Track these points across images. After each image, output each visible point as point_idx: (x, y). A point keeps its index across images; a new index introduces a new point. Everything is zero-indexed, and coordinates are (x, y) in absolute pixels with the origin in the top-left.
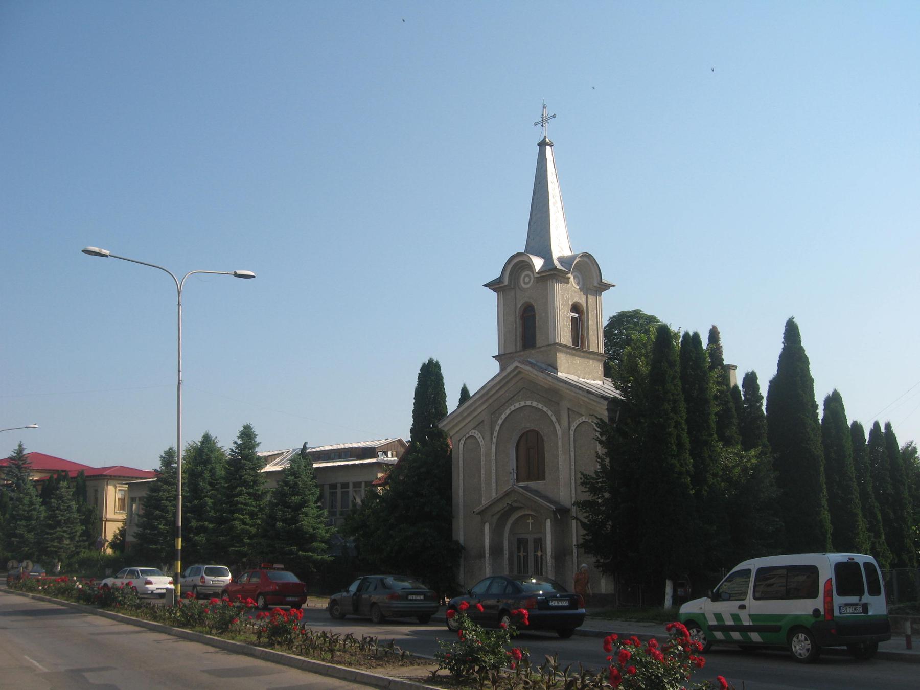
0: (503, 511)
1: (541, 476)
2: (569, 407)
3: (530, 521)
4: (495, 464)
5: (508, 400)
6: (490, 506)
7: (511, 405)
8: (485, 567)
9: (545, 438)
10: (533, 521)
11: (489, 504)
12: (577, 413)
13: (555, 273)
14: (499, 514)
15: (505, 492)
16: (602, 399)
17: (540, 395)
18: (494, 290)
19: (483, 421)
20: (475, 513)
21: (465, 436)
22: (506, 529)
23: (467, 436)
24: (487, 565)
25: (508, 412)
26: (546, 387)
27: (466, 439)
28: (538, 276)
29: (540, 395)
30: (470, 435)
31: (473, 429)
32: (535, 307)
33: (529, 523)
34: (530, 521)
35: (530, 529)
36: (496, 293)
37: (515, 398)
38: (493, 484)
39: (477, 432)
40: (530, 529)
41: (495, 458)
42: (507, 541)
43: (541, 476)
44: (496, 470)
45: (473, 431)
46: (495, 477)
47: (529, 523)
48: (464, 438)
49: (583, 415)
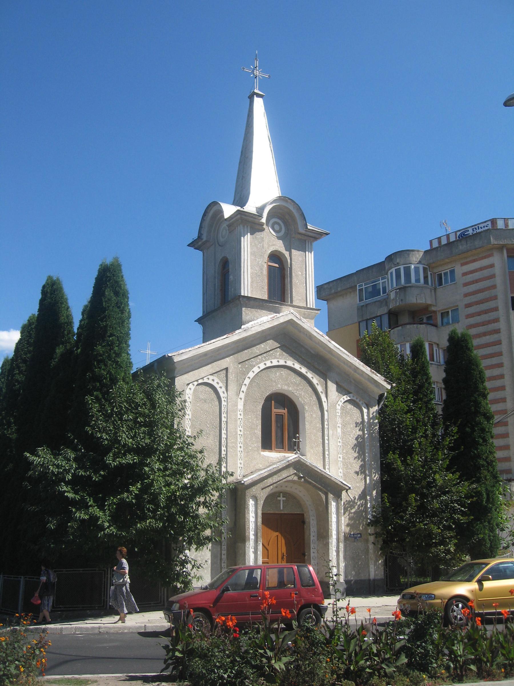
2: (338, 380)
3: (281, 499)
7: (266, 360)
10: (284, 499)
12: (345, 389)
17: (303, 359)
19: (227, 369)
21: (197, 381)
23: (200, 381)
26: (312, 352)
27: (198, 385)
29: (303, 359)
30: (206, 380)
31: (210, 375)
33: (280, 500)
34: (281, 499)
35: (282, 508)
37: (271, 352)
39: (216, 380)
40: (282, 508)
45: (211, 377)
47: (280, 500)
48: (196, 383)
49: (351, 393)
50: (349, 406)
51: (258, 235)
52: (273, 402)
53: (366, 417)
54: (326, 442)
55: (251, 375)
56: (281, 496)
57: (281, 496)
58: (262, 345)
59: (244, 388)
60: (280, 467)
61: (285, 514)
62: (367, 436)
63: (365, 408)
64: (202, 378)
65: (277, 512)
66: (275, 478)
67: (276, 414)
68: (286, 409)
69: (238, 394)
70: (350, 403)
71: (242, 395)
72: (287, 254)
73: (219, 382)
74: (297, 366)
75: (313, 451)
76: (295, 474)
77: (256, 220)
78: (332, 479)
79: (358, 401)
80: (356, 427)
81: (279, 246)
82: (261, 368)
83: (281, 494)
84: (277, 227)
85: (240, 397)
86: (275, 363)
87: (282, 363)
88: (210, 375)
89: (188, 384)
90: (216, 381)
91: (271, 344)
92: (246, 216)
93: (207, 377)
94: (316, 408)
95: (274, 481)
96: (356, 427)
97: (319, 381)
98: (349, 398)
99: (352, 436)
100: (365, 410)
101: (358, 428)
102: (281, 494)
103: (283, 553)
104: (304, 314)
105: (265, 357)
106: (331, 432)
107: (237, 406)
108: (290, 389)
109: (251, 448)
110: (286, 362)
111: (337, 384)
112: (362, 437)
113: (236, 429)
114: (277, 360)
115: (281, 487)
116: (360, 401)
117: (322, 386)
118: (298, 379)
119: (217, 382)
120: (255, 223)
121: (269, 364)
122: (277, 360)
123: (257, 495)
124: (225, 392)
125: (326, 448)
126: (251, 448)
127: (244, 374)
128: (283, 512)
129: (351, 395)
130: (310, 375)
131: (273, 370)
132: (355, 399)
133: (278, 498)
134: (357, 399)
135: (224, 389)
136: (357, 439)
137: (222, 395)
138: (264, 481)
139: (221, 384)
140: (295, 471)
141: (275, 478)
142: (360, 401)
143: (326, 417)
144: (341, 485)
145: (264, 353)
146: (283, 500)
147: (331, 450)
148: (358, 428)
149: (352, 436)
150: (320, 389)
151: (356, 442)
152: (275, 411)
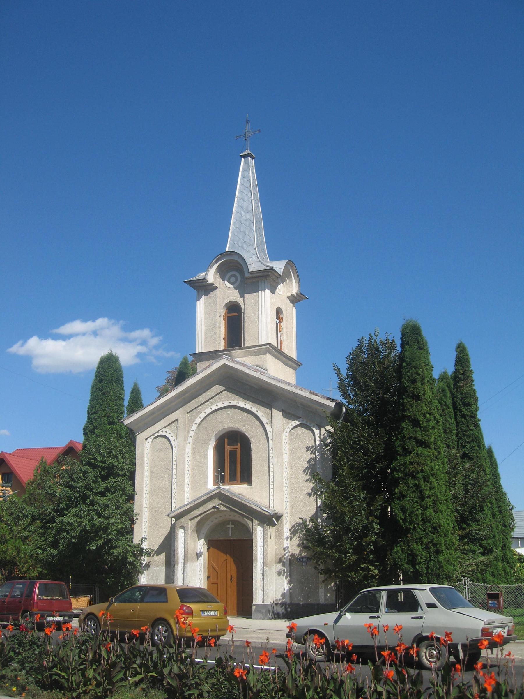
0: (203, 515)
1: (246, 478)
2: (283, 408)
3: (230, 526)
5: (210, 399)
7: (212, 404)
9: (252, 441)
10: (233, 526)
12: (294, 415)
13: (270, 273)
14: (199, 518)
16: (329, 401)
17: (248, 395)
18: (195, 288)
19: (177, 420)
20: (170, 516)
21: (153, 435)
23: (156, 435)
25: (208, 411)
27: (155, 438)
28: (249, 276)
29: (248, 395)
30: (160, 433)
31: (163, 428)
32: (242, 307)
33: (229, 528)
34: (230, 526)
35: (230, 535)
36: (196, 291)
37: (217, 397)
40: (230, 535)
43: (246, 478)
45: (164, 430)
47: (229, 528)
48: (153, 437)
49: (300, 418)
50: (301, 430)
51: (212, 294)
52: (226, 440)
53: (318, 439)
54: (271, 469)
55: (198, 421)
56: (230, 524)
57: (230, 524)
58: (208, 393)
59: (192, 434)
61: (234, 540)
62: (318, 457)
63: (316, 429)
64: (157, 432)
65: (226, 539)
66: (201, 510)
67: (229, 451)
68: (239, 445)
69: (185, 439)
70: (302, 427)
71: (190, 440)
72: (240, 300)
73: (171, 432)
74: (242, 403)
76: (221, 504)
77: (204, 283)
78: (253, 506)
79: (308, 424)
80: (307, 451)
81: (234, 296)
82: (207, 413)
83: (230, 522)
84: (233, 279)
85: (188, 442)
86: (220, 405)
87: (227, 404)
88: (163, 428)
89: (146, 439)
90: (168, 432)
91: (217, 388)
92: (193, 283)
93: (161, 430)
94: (263, 439)
95: (201, 512)
96: (307, 451)
97: (265, 413)
98: (297, 423)
99: (302, 460)
100: (317, 432)
101: (309, 452)
102: (230, 522)
103: (232, 576)
104: (255, 352)
105: (211, 403)
106: (275, 460)
107: (185, 450)
108: (237, 426)
110: (230, 402)
111: (283, 411)
112: (314, 459)
113: (184, 469)
114: (222, 402)
115: (225, 516)
116: (310, 424)
117: (268, 417)
118: (245, 415)
119: (167, 432)
120: (205, 286)
121: (214, 408)
122: (222, 402)
123: (182, 525)
124: (176, 440)
125: (271, 476)
127: (192, 421)
128: (232, 539)
129: (300, 419)
130: (254, 410)
131: (220, 412)
132: (304, 422)
133: (228, 526)
134: (307, 422)
135: (174, 438)
136: (309, 462)
137: (173, 443)
138: (191, 512)
139: (172, 435)
140: (221, 502)
141: (201, 510)
142: (310, 424)
143: (271, 446)
144: (261, 512)
145: (210, 399)
147: (275, 477)
148: (309, 452)
149: (302, 460)
150: (264, 420)
151: (308, 465)
152: (227, 448)
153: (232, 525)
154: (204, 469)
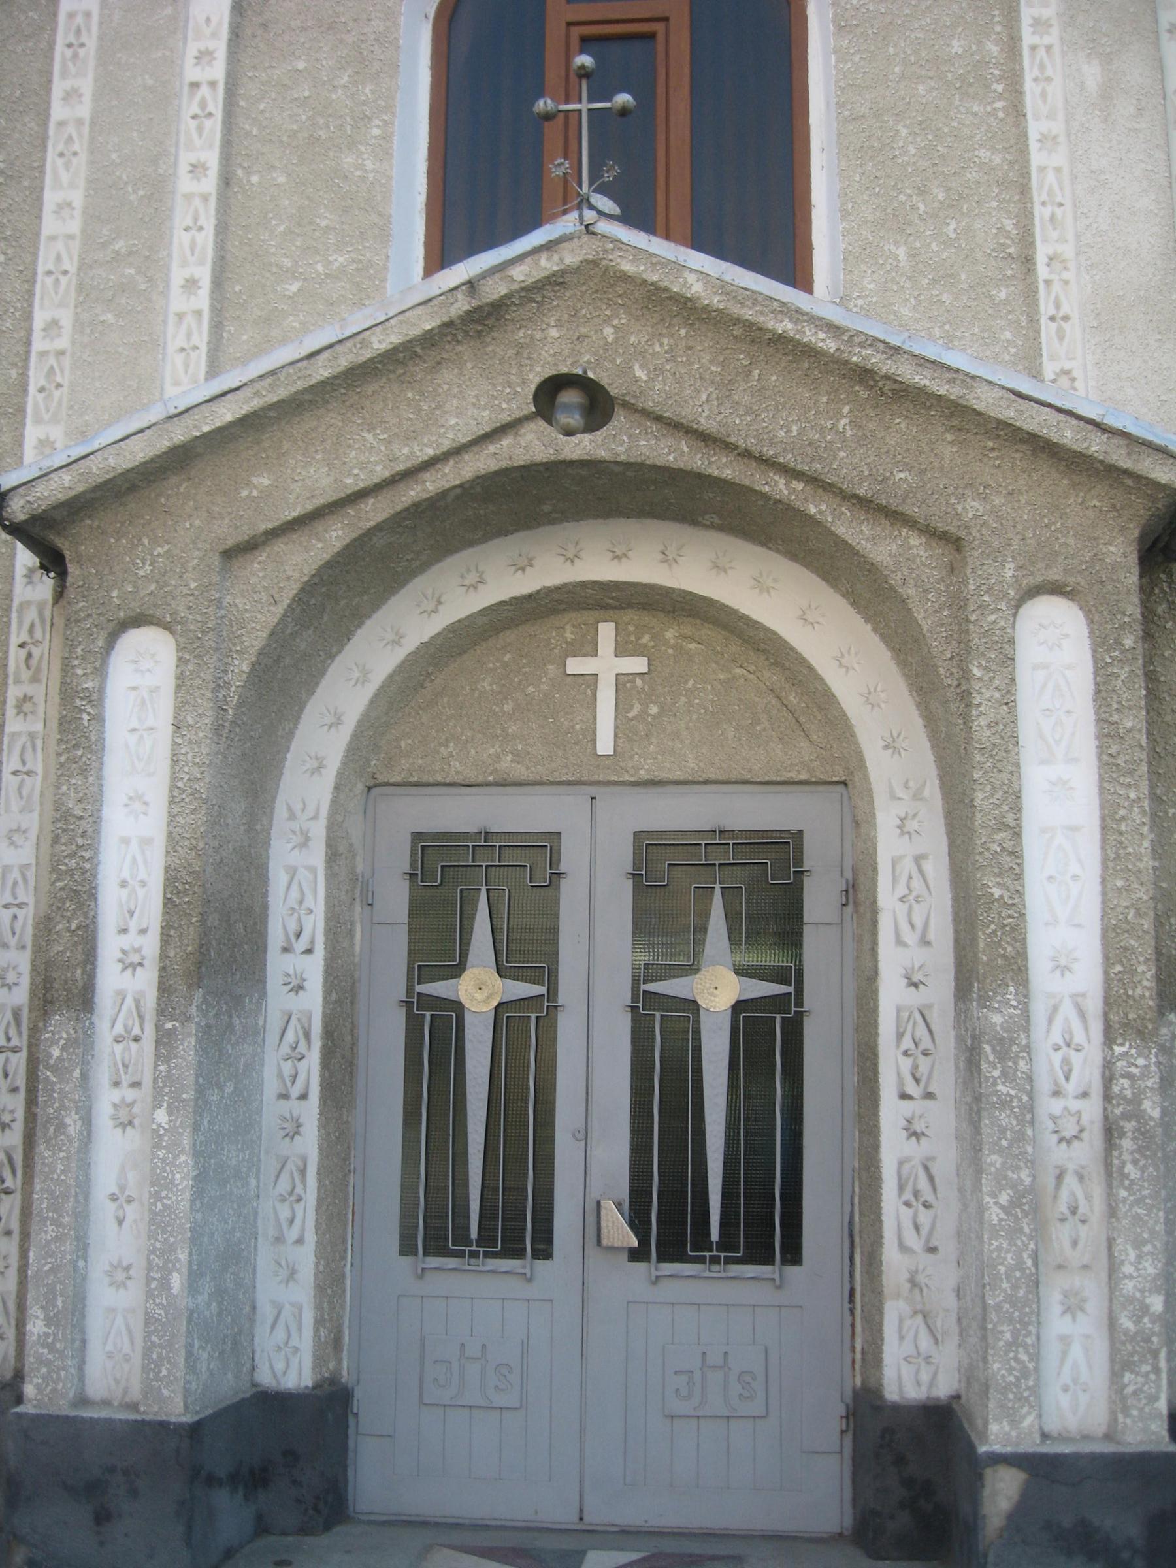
0: (375, 512)
4: (215, 126)
6: (250, 423)
8: (87, 1121)
10: (638, 665)
11: (227, 413)
15: (471, 285)
22: (315, 711)
24: (106, 1100)
35: (605, 744)
38: (178, 302)
40: (605, 744)
41: (218, 70)
42: (317, 856)
44: (226, 180)
46: (206, 238)
60: (380, 343)
75: (913, 255)
95: (353, 482)
109: (294, 287)
126: (294, 287)
133: (575, 665)
146: (623, 682)
153: (621, 651)
154: (349, 160)
